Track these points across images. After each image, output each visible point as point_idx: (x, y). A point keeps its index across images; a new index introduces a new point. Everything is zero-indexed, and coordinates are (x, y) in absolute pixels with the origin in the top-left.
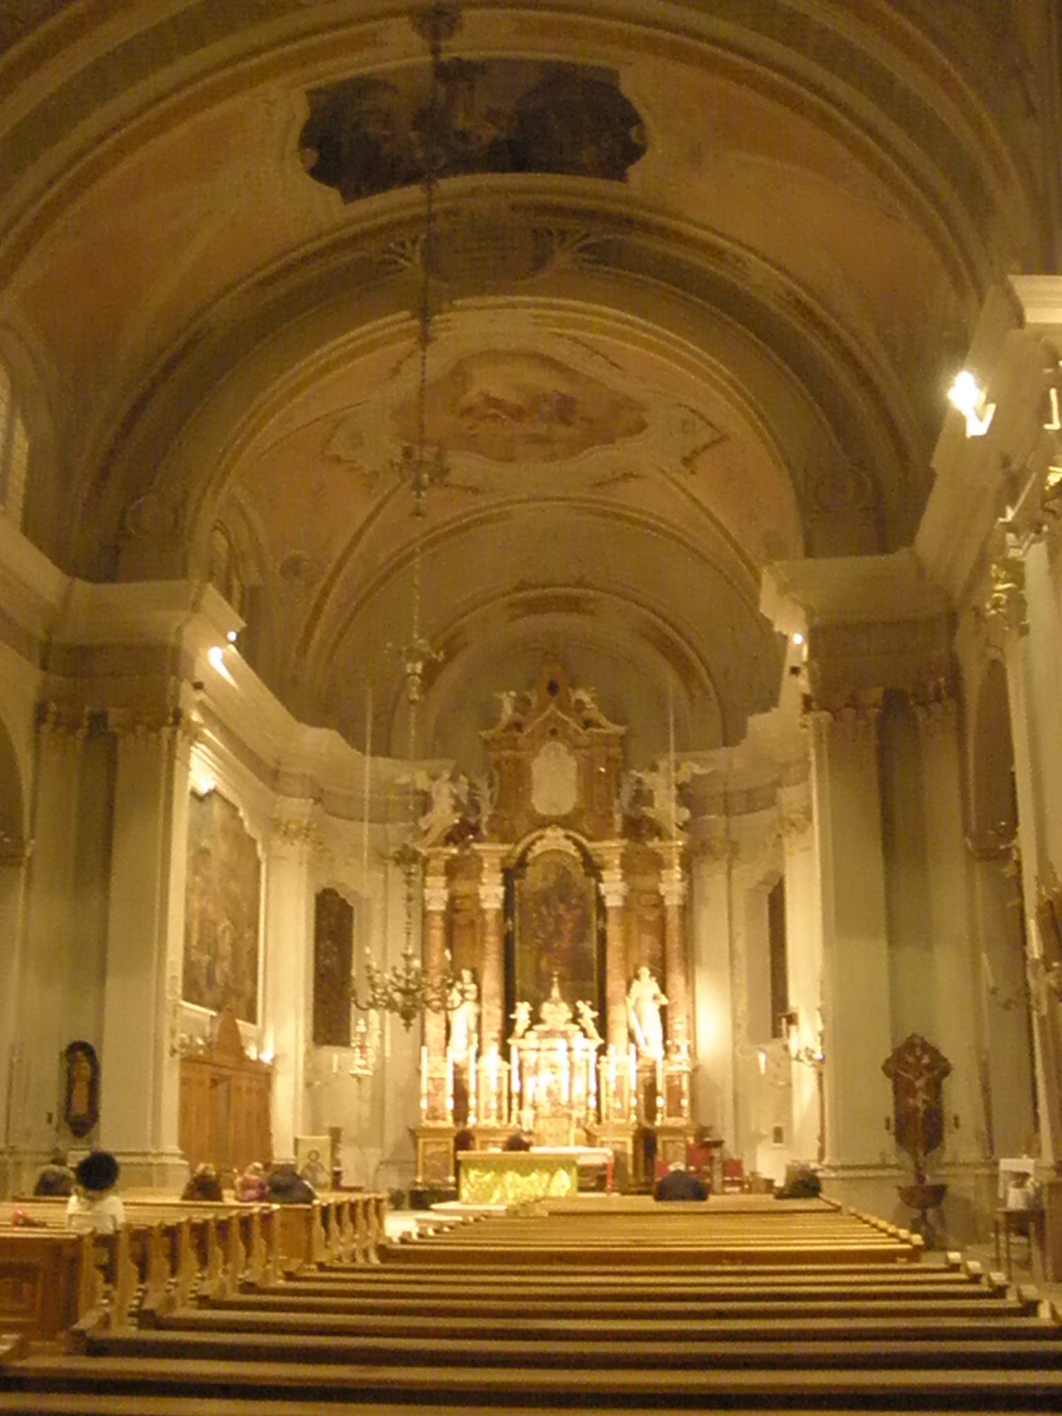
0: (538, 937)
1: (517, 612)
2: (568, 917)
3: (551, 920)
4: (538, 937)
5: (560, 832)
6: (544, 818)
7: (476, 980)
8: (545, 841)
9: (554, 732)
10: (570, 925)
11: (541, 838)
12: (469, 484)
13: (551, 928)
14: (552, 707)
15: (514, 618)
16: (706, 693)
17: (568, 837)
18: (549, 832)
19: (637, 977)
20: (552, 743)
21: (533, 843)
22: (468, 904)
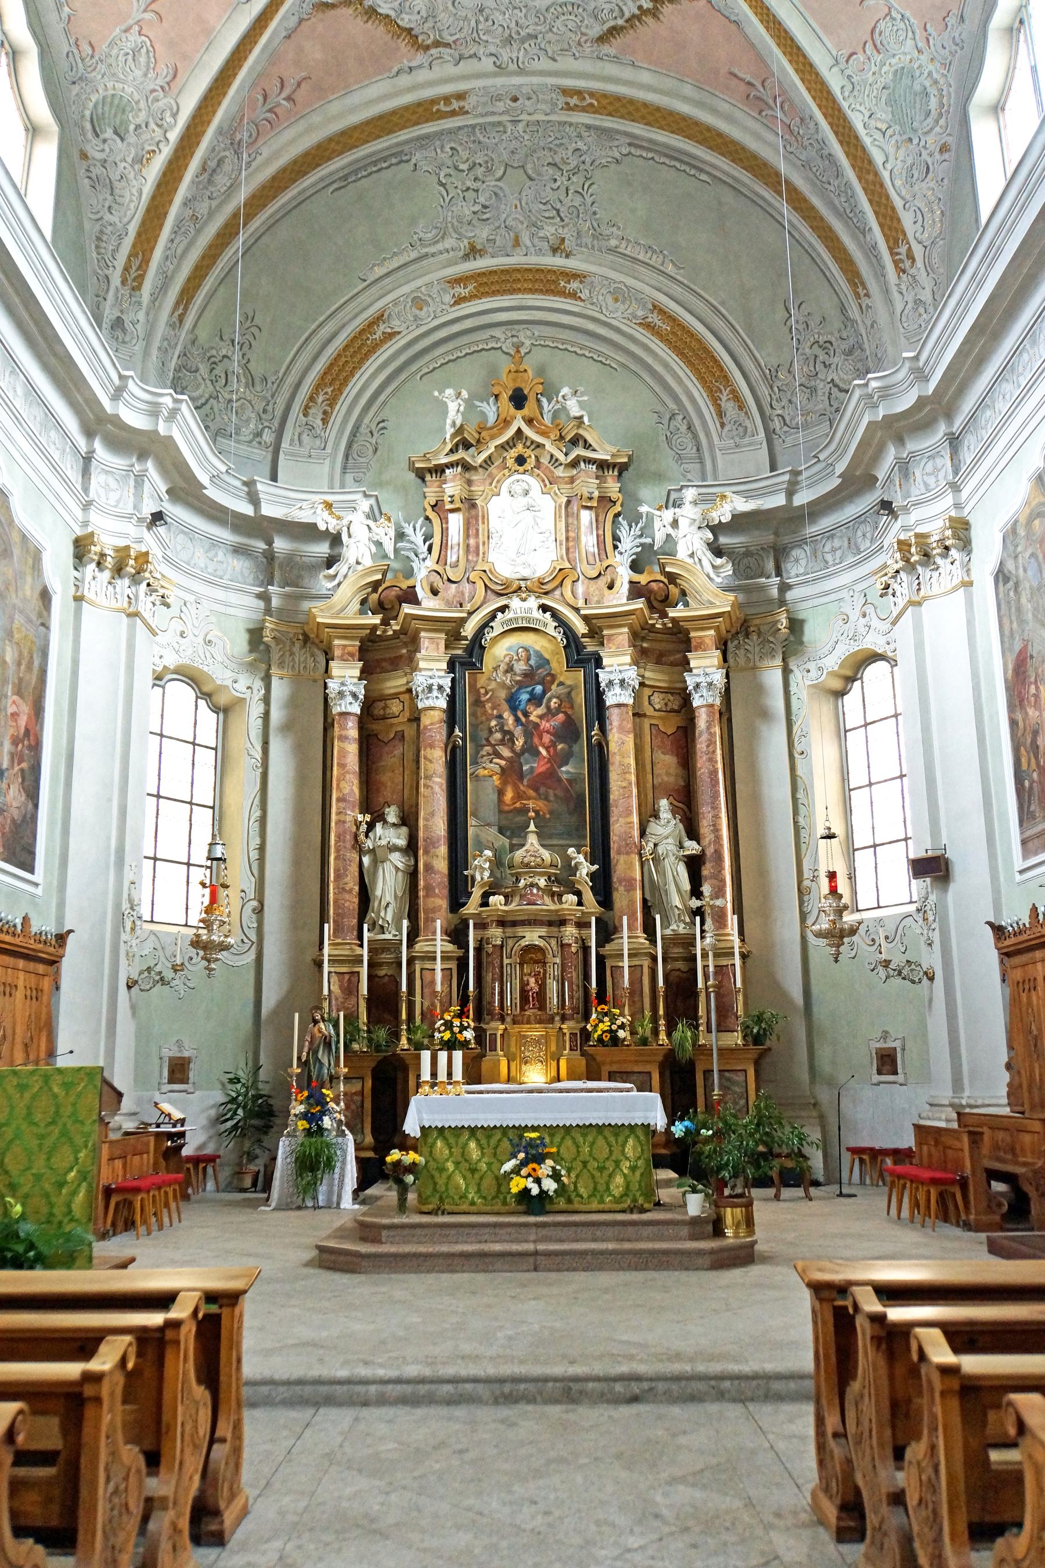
0: (499, 756)
1: (463, 292)
2: (545, 725)
3: (518, 731)
4: (499, 756)
5: (533, 603)
6: (507, 584)
7: (409, 820)
8: (509, 615)
9: (521, 460)
10: (547, 738)
11: (503, 609)
12: (405, 21)
13: (519, 743)
14: (519, 423)
15: (459, 300)
16: (741, 406)
17: (544, 608)
18: (515, 603)
19: (656, 816)
20: (517, 477)
21: (493, 617)
22: (395, 707)
